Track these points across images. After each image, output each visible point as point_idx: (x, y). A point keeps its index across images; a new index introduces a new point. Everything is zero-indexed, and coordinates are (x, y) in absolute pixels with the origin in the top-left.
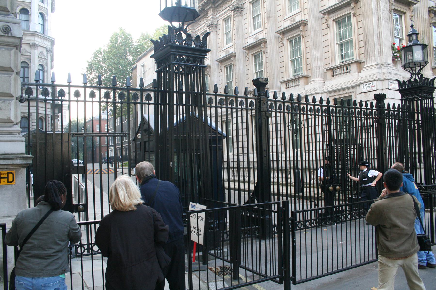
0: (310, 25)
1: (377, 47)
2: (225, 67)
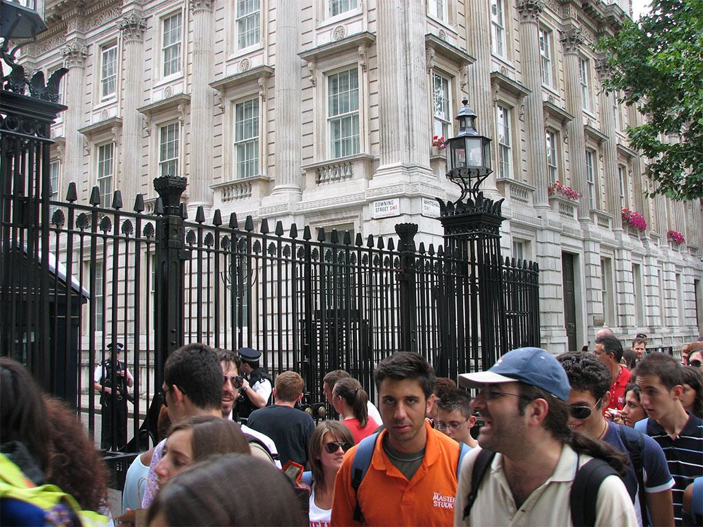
0: (278, 79)
1: (403, 133)
2: (96, 145)
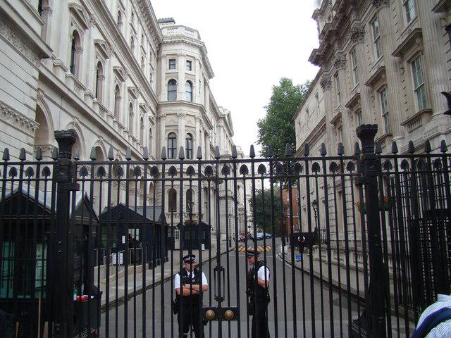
0: (428, 35)
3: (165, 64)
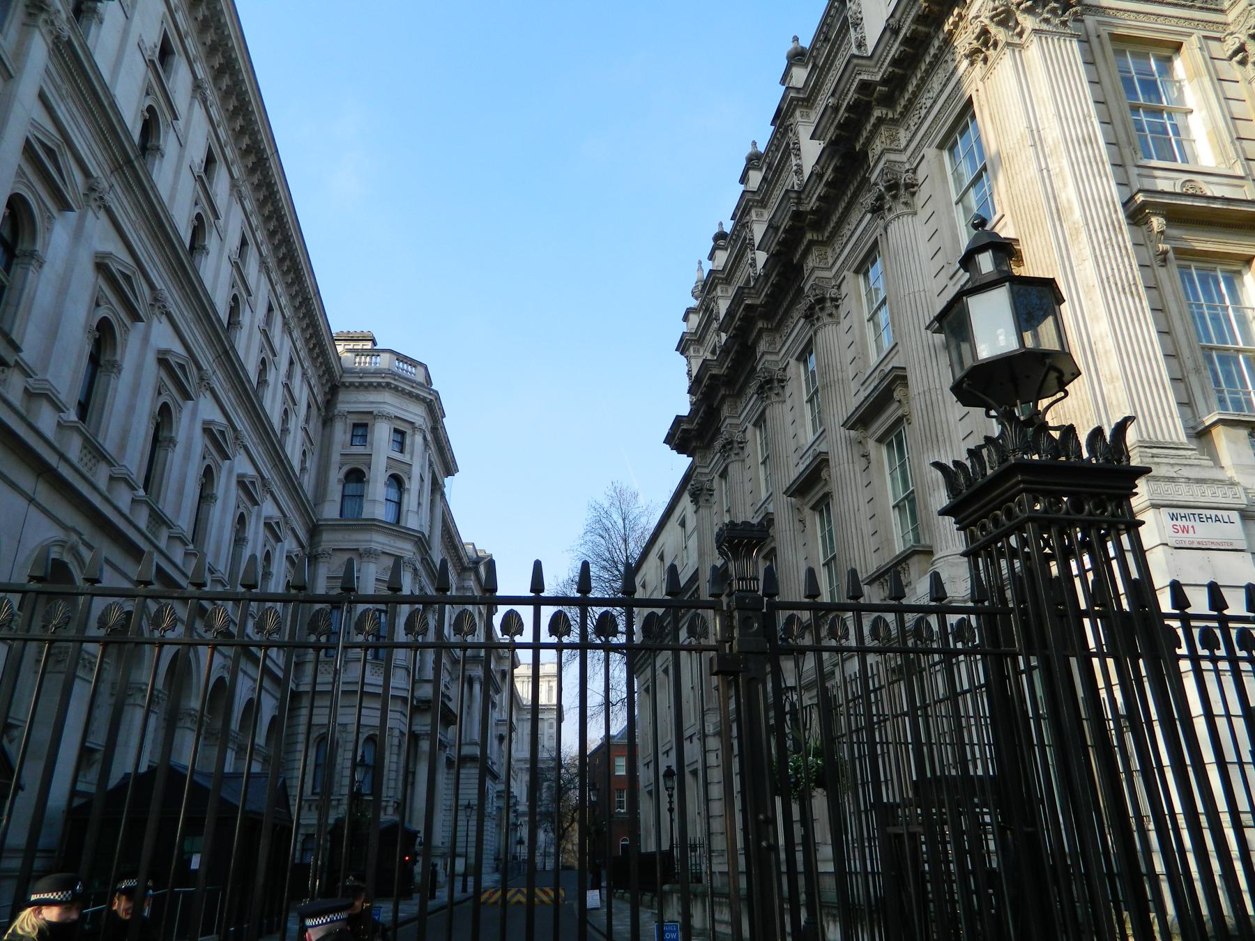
3: (341, 433)
